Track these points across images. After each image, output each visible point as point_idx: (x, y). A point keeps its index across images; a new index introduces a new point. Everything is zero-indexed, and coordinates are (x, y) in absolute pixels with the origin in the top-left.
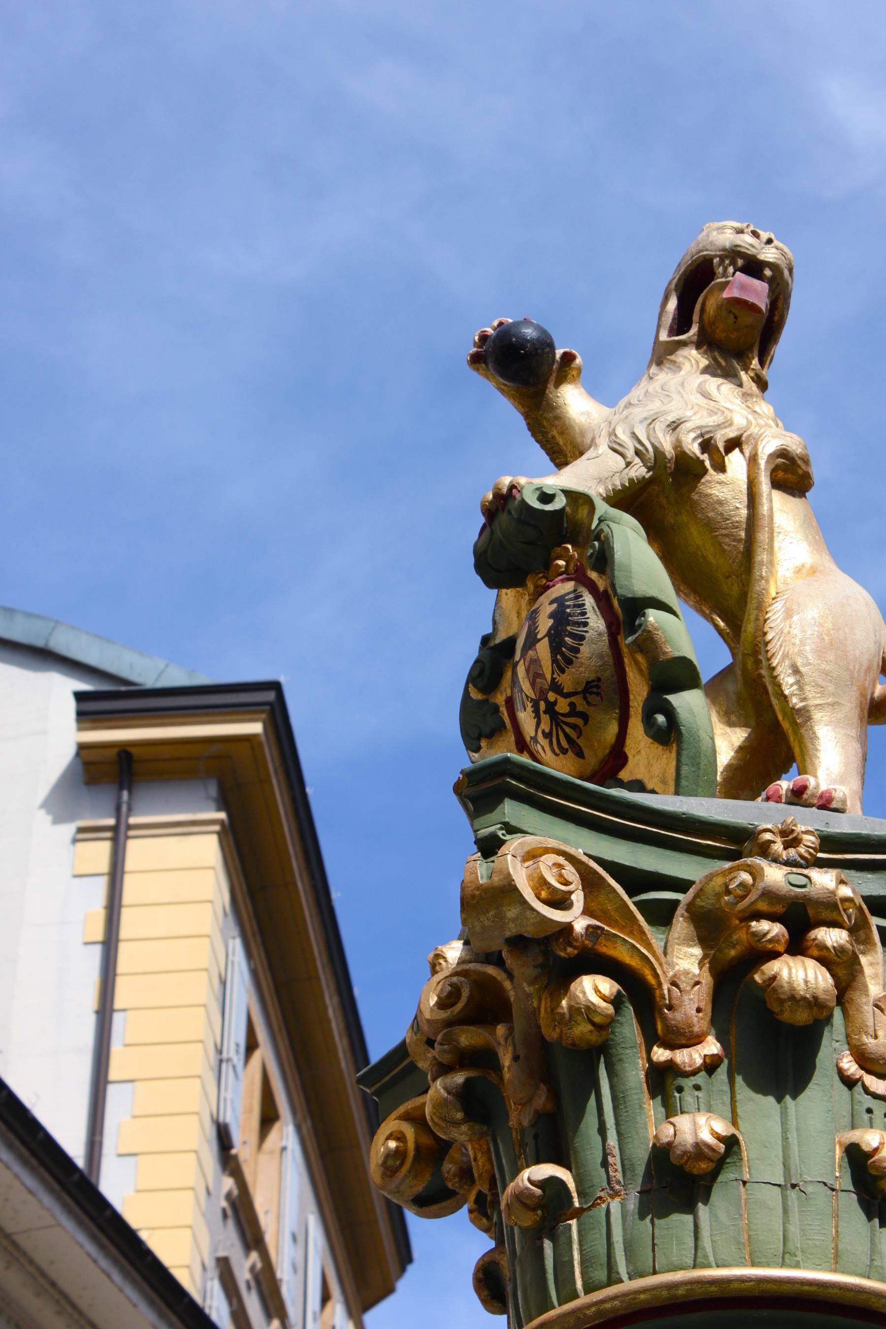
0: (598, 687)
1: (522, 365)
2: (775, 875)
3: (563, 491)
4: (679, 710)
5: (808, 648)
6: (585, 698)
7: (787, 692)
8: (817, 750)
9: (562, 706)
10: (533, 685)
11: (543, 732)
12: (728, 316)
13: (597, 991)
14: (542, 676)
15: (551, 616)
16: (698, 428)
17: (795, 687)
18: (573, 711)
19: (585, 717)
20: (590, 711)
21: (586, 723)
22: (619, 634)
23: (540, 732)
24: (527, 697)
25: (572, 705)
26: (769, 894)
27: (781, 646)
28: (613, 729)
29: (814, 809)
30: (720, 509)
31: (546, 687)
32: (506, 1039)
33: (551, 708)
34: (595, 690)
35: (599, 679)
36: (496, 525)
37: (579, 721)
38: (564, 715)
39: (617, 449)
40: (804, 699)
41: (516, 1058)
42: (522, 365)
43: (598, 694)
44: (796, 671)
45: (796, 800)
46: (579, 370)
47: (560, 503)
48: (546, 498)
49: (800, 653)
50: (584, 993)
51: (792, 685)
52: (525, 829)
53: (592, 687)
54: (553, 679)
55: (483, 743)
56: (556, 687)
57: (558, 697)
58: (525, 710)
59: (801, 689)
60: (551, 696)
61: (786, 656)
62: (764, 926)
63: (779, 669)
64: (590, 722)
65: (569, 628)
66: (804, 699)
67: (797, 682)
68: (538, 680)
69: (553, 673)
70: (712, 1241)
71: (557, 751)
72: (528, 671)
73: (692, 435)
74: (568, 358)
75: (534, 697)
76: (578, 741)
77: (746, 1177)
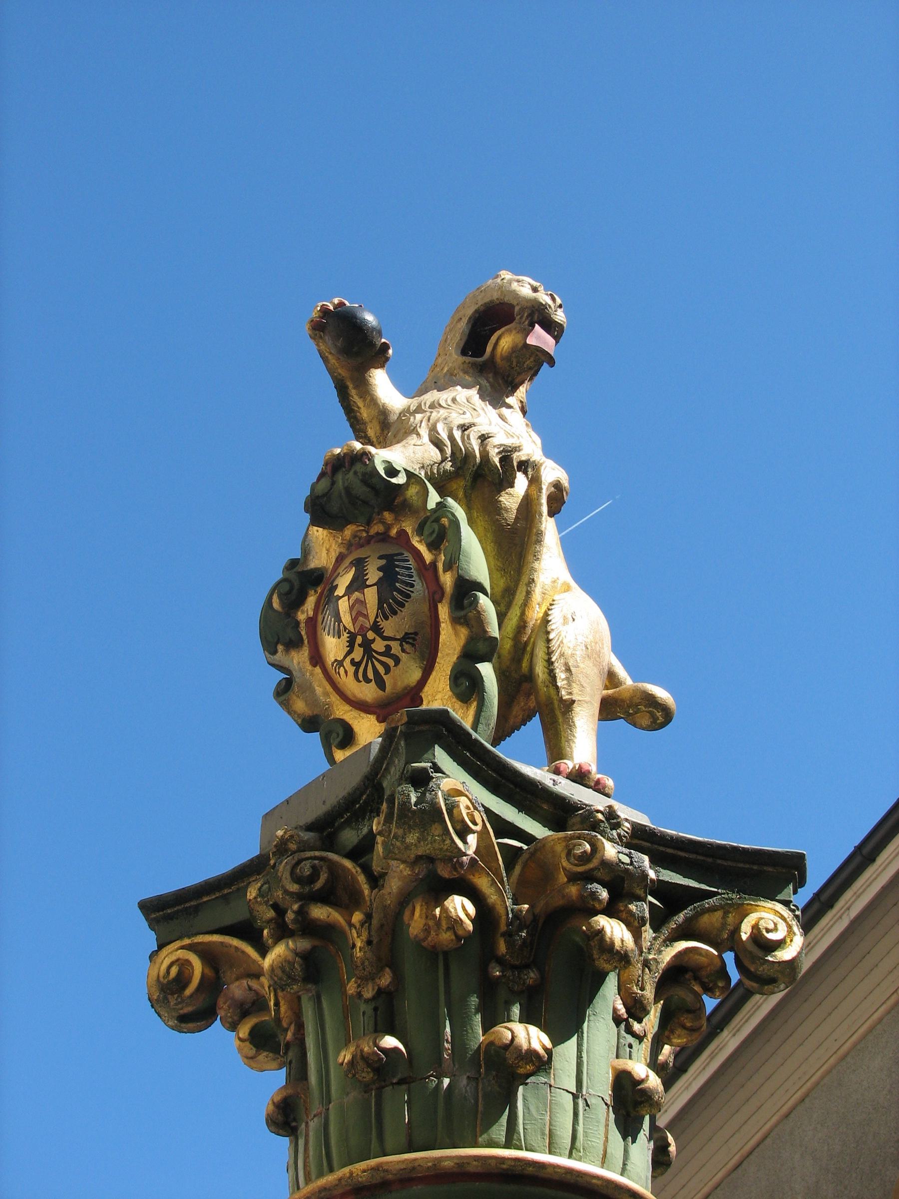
0: (414, 639)
1: (351, 344)
2: (611, 851)
3: (405, 470)
4: (485, 679)
5: (578, 653)
6: (401, 645)
7: (559, 684)
8: (574, 736)
9: (379, 645)
10: (354, 621)
11: (352, 660)
12: (493, 347)
13: (463, 907)
14: (366, 616)
15: (380, 569)
16: (501, 445)
17: (565, 682)
18: (388, 652)
19: (397, 661)
20: (403, 657)
21: (395, 666)
22: (440, 601)
23: (348, 660)
24: (345, 628)
25: (388, 648)
26: (606, 864)
27: (559, 646)
28: (416, 675)
29: (591, 790)
30: (505, 515)
31: (368, 626)
32: (362, 925)
33: (367, 645)
34: (411, 641)
35: (416, 634)
36: (339, 477)
37: (391, 662)
38: (375, 652)
39: (437, 443)
40: (570, 693)
41: (369, 942)
42: (351, 344)
43: (413, 645)
44: (568, 670)
45: (578, 779)
46: (387, 359)
47: (401, 479)
48: (392, 471)
49: (573, 655)
50: (456, 909)
51: (563, 680)
52: (444, 770)
53: (409, 638)
54: (376, 622)
55: (280, 648)
56: (376, 628)
57: (377, 637)
58: (339, 637)
59: (569, 685)
60: (371, 635)
61: (562, 655)
62: (596, 887)
63: (556, 664)
64: (400, 666)
65: (397, 584)
66: (570, 693)
67: (567, 679)
68: (361, 618)
69: (377, 617)
70: (524, 1128)
71: (361, 678)
72: (351, 608)
73: (497, 450)
74: (385, 347)
75: (353, 631)
76: (384, 677)
77: (552, 1083)
